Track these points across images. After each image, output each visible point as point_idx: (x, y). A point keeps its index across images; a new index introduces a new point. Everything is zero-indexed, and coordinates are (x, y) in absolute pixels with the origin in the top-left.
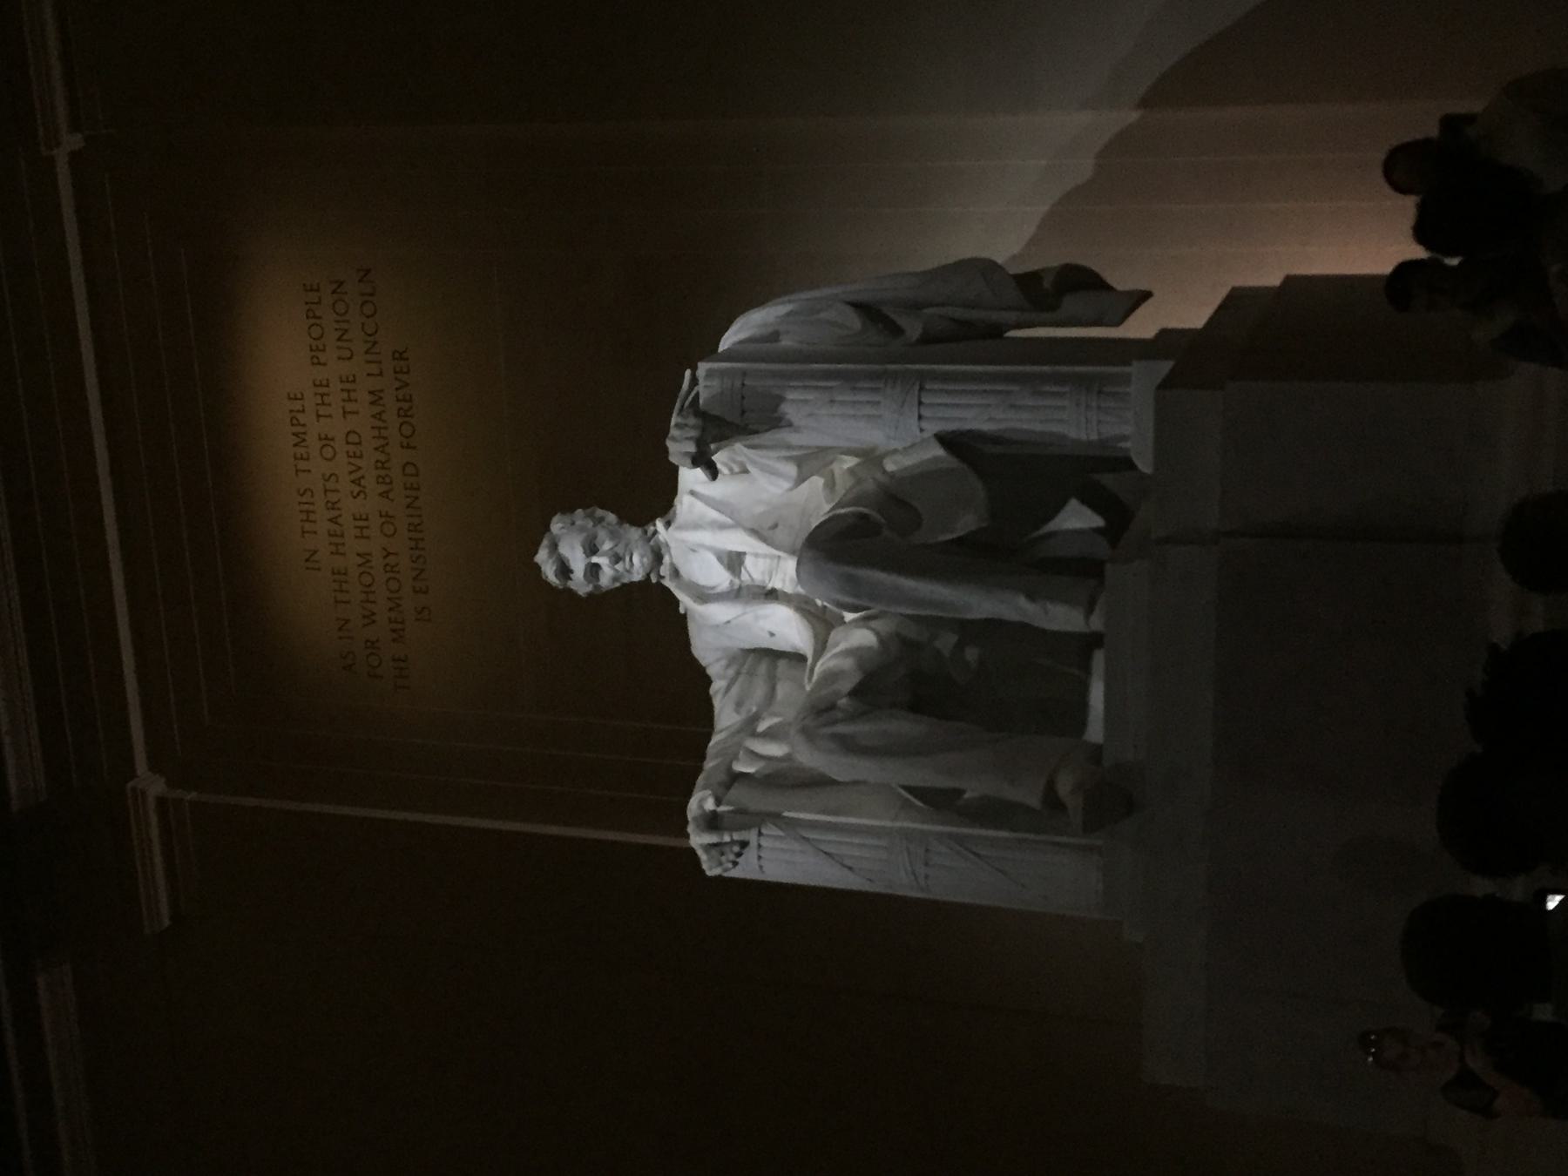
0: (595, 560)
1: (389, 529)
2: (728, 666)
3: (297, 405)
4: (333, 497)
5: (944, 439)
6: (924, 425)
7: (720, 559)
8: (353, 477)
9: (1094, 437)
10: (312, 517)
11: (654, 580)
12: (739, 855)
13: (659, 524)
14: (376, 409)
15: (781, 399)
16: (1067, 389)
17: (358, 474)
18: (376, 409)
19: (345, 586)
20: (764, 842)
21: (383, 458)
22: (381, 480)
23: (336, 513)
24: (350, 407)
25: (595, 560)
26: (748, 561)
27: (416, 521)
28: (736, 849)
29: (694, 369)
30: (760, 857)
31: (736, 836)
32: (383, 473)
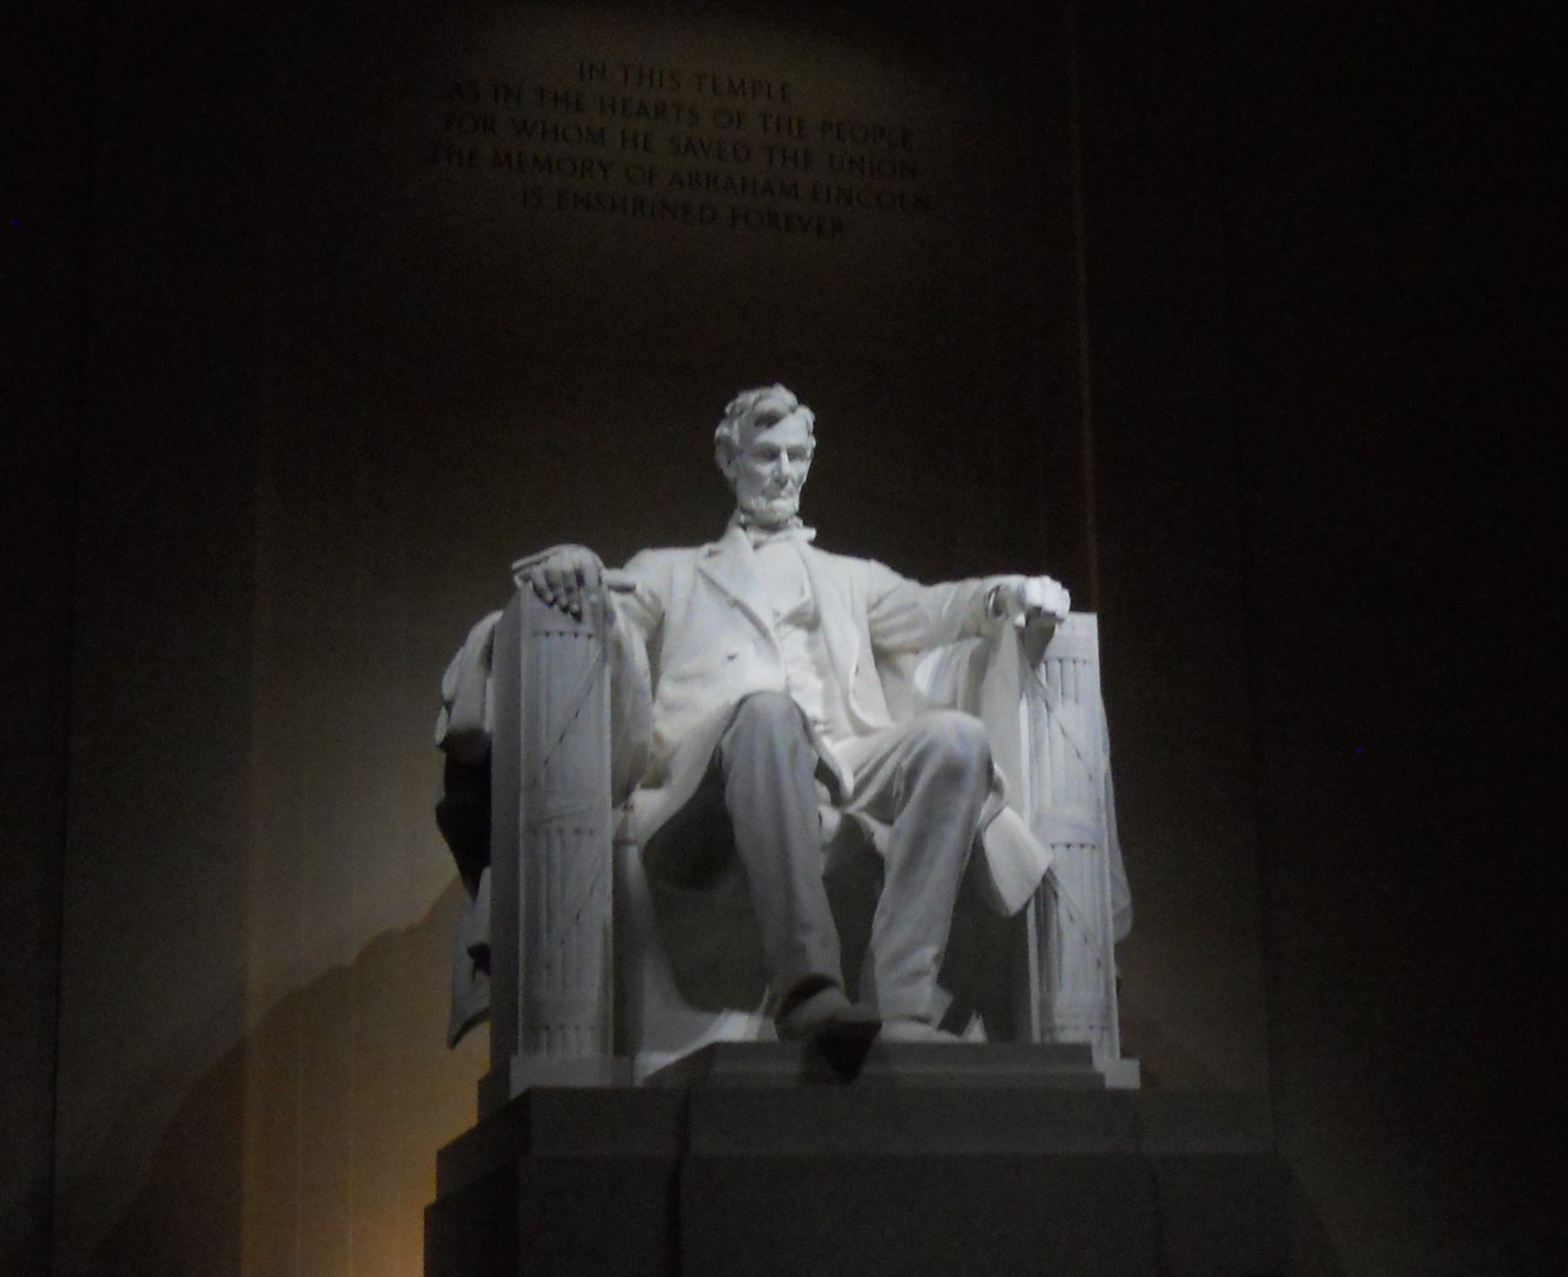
0: (784, 456)
2: (654, 596)
5: (1049, 870)
6: (1060, 851)
7: (806, 604)
9: (1058, 1021)
12: (565, 610)
13: (812, 533)
15: (1077, 700)
16: (1102, 994)
20: (582, 639)
25: (784, 456)
26: (801, 635)
28: (575, 607)
30: (561, 634)
31: (586, 608)
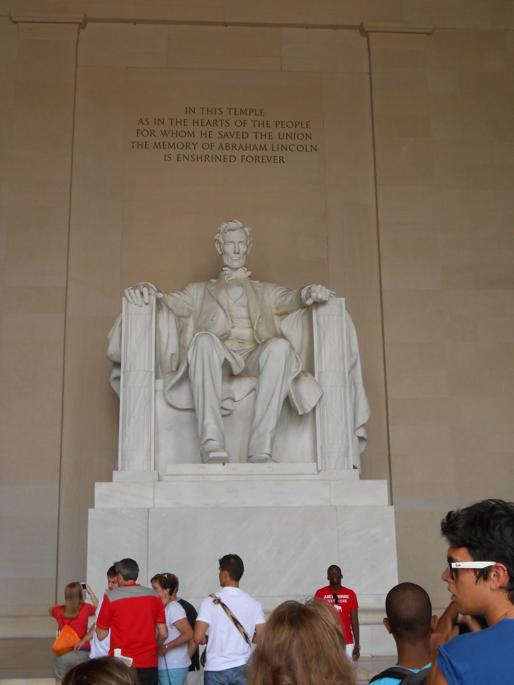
1: (206, 146)
3: (258, 112)
4: (219, 123)
8: (229, 134)
10: (210, 113)
11: (224, 269)
13: (249, 273)
14: (258, 148)
17: (230, 136)
18: (258, 148)
19: (179, 124)
21: (237, 147)
22: (227, 146)
23: (212, 124)
24: (259, 136)
27: (210, 159)
29: (337, 295)
32: (231, 146)
